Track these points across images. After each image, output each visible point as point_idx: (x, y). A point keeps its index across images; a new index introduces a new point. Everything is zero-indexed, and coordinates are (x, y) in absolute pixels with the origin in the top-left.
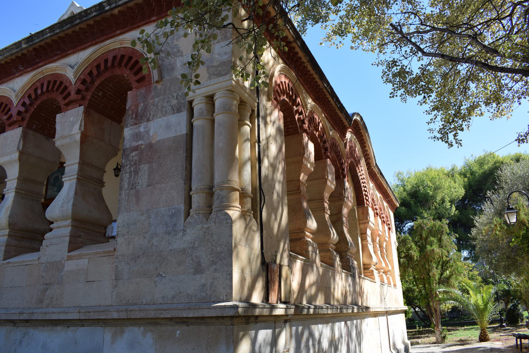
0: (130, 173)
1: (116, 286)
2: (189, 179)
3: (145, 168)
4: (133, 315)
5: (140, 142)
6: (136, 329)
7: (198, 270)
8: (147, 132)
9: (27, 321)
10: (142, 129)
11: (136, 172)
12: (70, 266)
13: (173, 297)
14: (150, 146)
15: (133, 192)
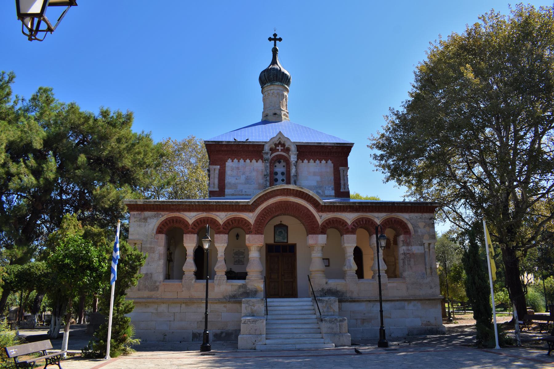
0: (408, 260)
1: (407, 291)
2: (425, 265)
3: (412, 260)
4: (417, 298)
5: (410, 252)
6: (415, 302)
7: (431, 288)
8: (412, 249)
9: (376, 300)
10: (410, 248)
11: (410, 261)
12: (389, 285)
13: (425, 294)
14: (413, 254)
15: (409, 266)
